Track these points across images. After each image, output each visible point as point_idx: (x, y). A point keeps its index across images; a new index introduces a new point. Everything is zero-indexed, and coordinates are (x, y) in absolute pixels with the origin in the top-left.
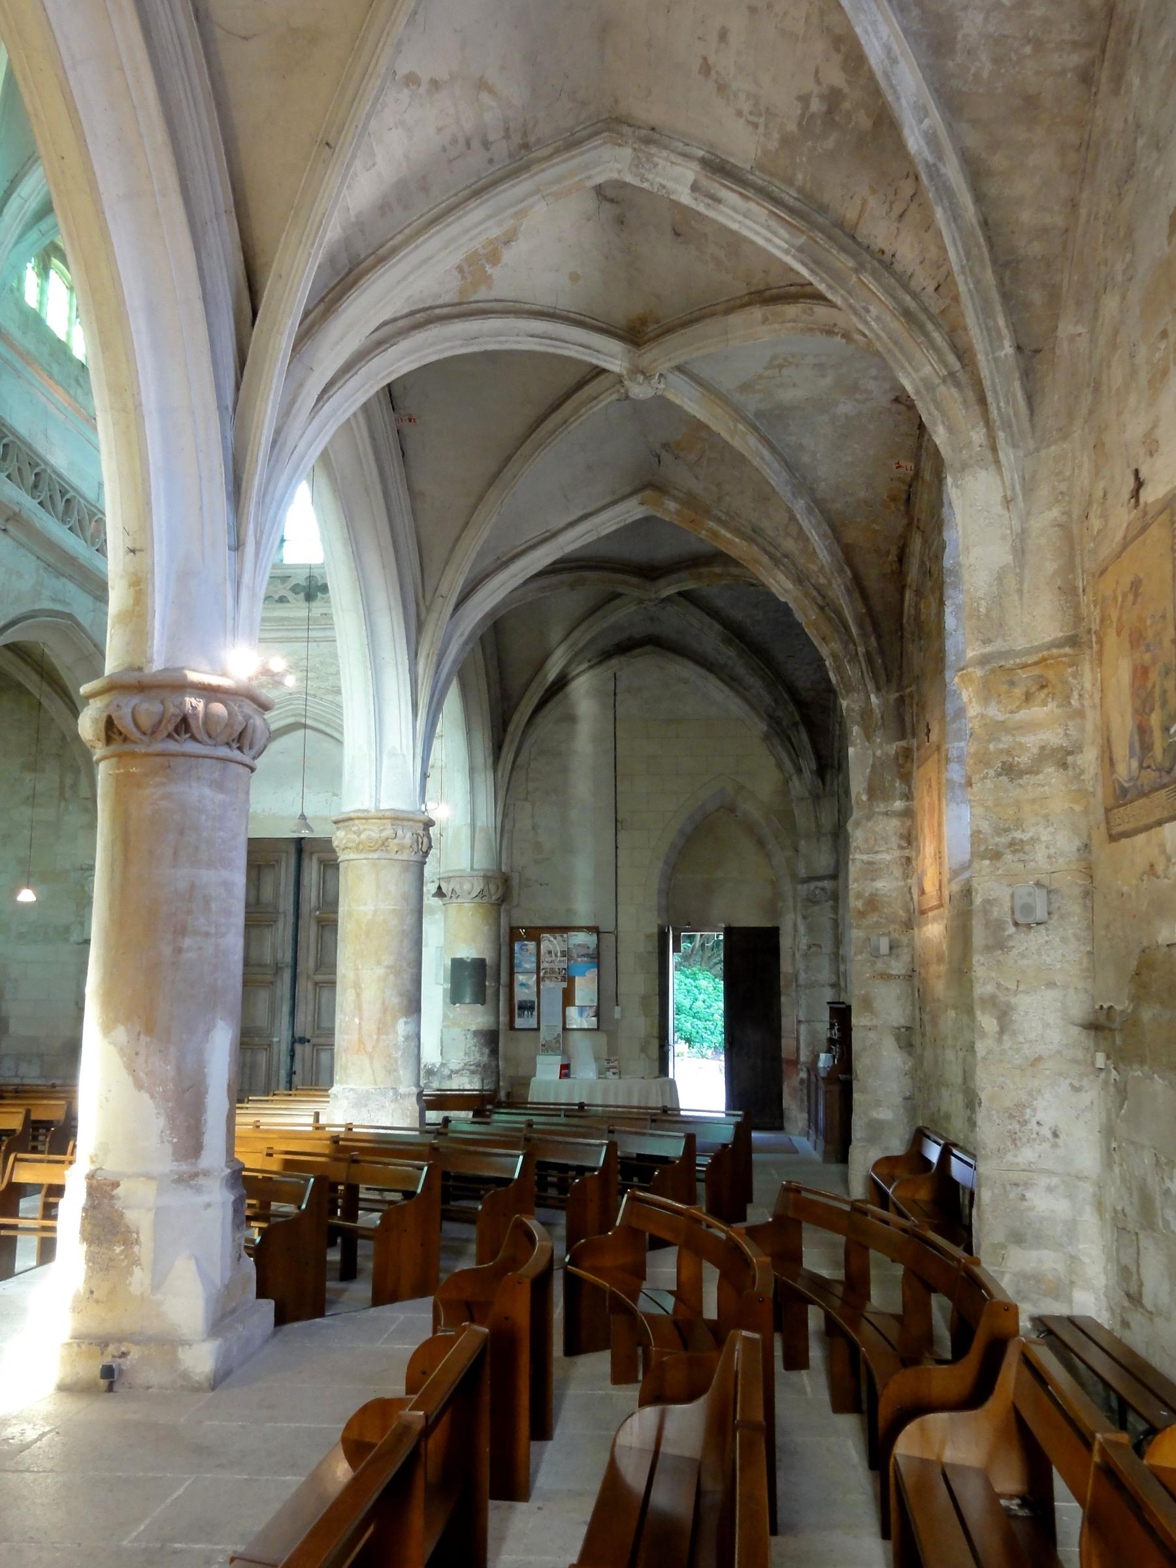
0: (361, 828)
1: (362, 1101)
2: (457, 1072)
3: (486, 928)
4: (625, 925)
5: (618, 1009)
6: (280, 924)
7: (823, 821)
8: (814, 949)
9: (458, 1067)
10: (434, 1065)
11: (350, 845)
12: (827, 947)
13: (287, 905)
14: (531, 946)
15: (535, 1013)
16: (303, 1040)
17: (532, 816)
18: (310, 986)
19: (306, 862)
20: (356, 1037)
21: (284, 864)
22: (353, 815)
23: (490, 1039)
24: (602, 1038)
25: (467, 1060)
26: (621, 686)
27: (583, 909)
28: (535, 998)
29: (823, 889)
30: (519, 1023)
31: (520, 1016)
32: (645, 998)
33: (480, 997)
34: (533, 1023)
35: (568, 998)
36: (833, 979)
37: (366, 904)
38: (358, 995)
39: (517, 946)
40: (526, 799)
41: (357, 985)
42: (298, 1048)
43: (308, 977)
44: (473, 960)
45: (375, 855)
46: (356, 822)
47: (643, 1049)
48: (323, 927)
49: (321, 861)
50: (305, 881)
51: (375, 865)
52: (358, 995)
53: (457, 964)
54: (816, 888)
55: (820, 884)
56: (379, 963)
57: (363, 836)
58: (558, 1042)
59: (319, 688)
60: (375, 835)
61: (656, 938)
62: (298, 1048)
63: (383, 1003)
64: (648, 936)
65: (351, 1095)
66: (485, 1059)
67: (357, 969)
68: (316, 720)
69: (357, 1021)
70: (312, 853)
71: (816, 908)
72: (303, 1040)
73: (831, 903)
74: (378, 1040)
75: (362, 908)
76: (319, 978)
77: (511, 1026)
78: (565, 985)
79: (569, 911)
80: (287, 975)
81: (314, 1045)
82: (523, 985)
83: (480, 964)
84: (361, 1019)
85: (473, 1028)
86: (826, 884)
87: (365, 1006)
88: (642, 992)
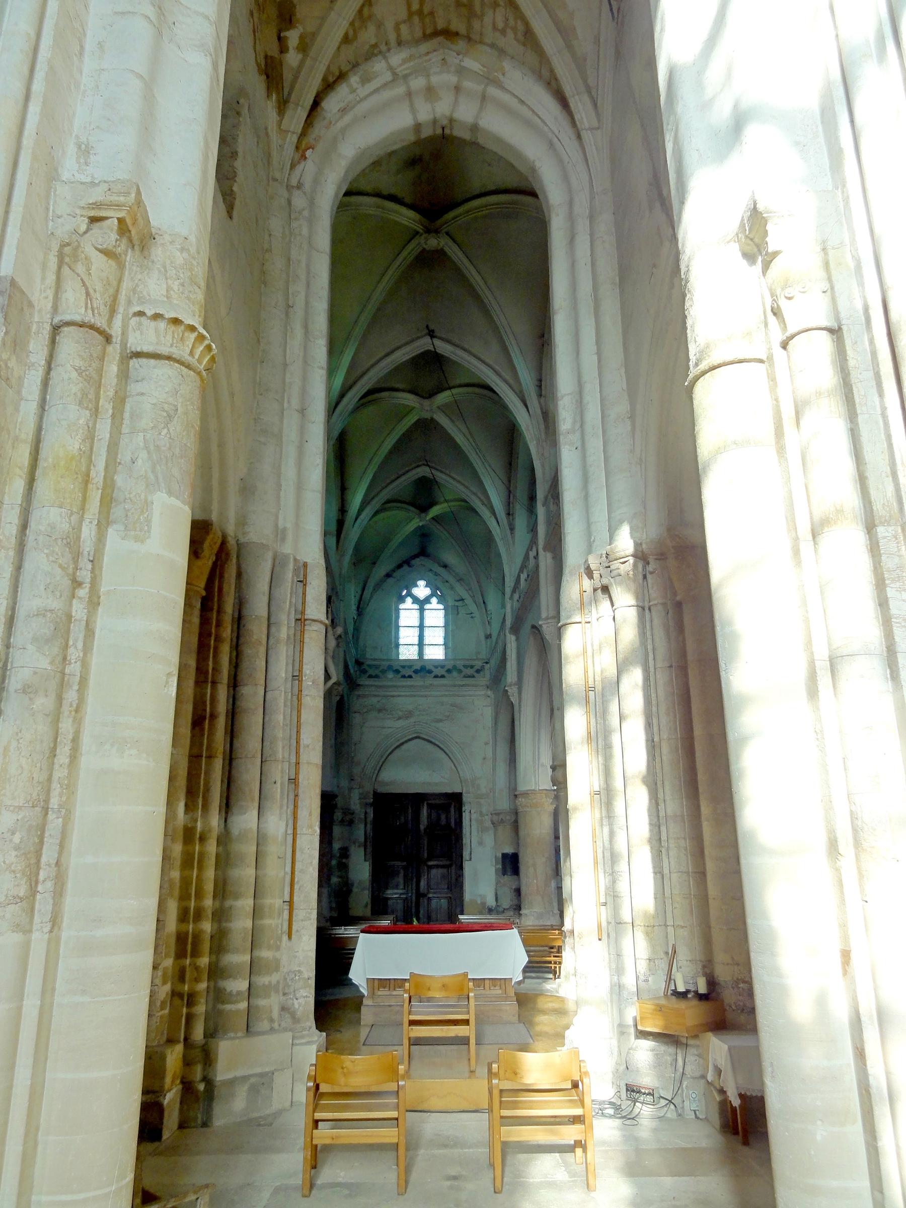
1: (540, 916)
38: (535, 870)
49: (428, 804)
53: (505, 856)
72: (424, 895)
76: (430, 863)
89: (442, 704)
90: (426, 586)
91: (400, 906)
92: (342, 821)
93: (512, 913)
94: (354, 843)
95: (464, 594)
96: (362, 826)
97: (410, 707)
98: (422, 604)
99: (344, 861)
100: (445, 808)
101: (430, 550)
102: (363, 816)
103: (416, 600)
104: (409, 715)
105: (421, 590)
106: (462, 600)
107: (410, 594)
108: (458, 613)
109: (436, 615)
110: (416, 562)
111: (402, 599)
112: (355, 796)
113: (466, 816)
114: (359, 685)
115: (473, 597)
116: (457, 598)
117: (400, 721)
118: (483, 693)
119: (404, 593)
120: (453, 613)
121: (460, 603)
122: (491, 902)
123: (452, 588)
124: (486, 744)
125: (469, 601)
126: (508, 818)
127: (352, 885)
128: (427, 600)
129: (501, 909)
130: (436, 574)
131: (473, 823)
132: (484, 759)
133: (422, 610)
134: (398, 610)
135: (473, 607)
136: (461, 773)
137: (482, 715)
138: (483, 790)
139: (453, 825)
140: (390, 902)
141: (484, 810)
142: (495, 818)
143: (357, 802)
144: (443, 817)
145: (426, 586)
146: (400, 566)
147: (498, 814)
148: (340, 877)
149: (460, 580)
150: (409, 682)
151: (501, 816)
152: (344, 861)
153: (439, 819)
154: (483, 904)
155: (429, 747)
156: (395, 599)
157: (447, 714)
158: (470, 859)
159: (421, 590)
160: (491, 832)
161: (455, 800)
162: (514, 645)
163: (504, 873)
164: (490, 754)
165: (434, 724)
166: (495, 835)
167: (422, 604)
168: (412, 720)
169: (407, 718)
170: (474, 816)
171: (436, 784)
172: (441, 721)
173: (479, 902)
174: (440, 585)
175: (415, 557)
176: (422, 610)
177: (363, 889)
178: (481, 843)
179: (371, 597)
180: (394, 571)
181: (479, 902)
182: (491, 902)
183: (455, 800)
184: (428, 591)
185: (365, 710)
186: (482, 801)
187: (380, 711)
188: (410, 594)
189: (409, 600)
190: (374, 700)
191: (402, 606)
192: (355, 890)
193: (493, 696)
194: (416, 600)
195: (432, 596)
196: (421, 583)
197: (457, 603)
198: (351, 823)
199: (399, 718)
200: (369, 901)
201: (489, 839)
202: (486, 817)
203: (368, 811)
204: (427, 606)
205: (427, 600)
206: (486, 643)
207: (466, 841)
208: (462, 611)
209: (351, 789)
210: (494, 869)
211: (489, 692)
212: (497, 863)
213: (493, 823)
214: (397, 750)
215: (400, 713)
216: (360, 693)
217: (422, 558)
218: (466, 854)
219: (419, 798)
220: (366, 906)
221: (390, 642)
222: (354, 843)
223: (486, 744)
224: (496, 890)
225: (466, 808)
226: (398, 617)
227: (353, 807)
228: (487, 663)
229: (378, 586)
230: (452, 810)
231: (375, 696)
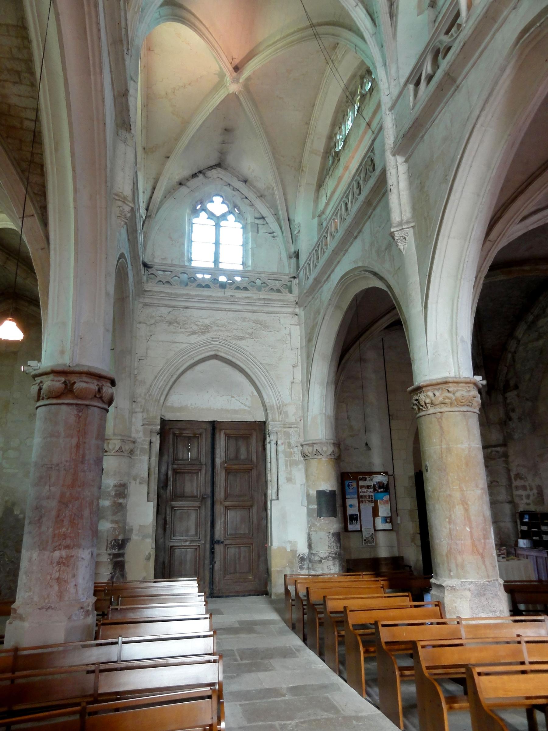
0: (456, 389)
2: (325, 558)
3: (333, 473)
4: (399, 472)
5: (399, 518)
6: (203, 471)
7: (491, 416)
8: (494, 483)
9: (325, 555)
10: (304, 554)
11: (447, 401)
12: (503, 481)
13: (205, 459)
14: (354, 484)
15: (359, 521)
16: (218, 542)
17: (347, 411)
18: (222, 509)
19: (217, 436)
20: (469, 542)
21: (204, 436)
22: (450, 380)
23: (338, 536)
24: (394, 535)
25: (330, 550)
26: (386, 346)
27: (377, 461)
28: (357, 513)
29: (497, 452)
30: (351, 527)
31: (350, 524)
32: (411, 511)
33: (334, 514)
34: (357, 527)
35: (375, 513)
36: (509, 498)
37: (462, 443)
38: (466, 510)
39: (347, 483)
40: (343, 402)
41: (464, 502)
42: (216, 547)
43: (221, 503)
44: (330, 491)
45: (465, 409)
46: (450, 385)
47: (413, 540)
48: (229, 473)
49: (226, 435)
50: (217, 446)
51: (465, 416)
52: (466, 510)
54: (492, 452)
55: (494, 449)
56: (477, 486)
57: (458, 394)
58: (372, 538)
59: (228, 336)
60: (466, 394)
61: (414, 478)
62: (216, 547)
63: (484, 516)
64: (410, 477)
65: (472, 587)
66: (338, 550)
67: (462, 490)
68: (226, 354)
69: (468, 529)
70: (221, 430)
71: (493, 462)
72: (218, 542)
73: (503, 459)
74: (485, 543)
75: (459, 446)
76: (227, 503)
77: (346, 529)
78: (373, 505)
79: (371, 464)
80: (209, 502)
81: (226, 545)
82: (351, 506)
83: (332, 493)
84: (471, 528)
85: (332, 531)
86: (499, 449)
87: (473, 518)
88: (409, 508)
89: (244, 320)
90: (223, 202)
91: (190, 554)
92: (120, 450)
93: (331, 563)
94: (135, 479)
95: (265, 212)
96: (146, 458)
97: (207, 322)
98: (218, 220)
99: (121, 501)
100: (246, 438)
101: (230, 159)
102: (147, 447)
103: (211, 215)
104: (206, 329)
105: (217, 206)
106: (263, 218)
107: (204, 209)
108: (258, 232)
109: (233, 232)
110: (213, 173)
111: (195, 212)
112: (138, 421)
113: (271, 449)
114: (146, 291)
115: (276, 215)
116: (257, 215)
117: (195, 336)
118: (290, 310)
119: (199, 207)
120: (255, 227)
121: (260, 222)
122: (303, 549)
123: (252, 205)
124: (294, 366)
125: (270, 219)
126: (325, 449)
127: (131, 530)
128: (224, 217)
129: (317, 558)
130: (235, 189)
131: (281, 455)
132: (293, 382)
133: (217, 226)
134: (191, 224)
135: (274, 226)
136: (265, 397)
137: (290, 334)
138: (292, 419)
139: (254, 458)
140: (177, 551)
141: (293, 440)
142: (308, 450)
143: (140, 428)
144: (243, 450)
145: (223, 202)
146: (194, 176)
147: (312, 445)
148: (113, 522)
149: (261, 196)
150: (206, 292)
151: (316, 447)
152: (121, 501)
153: (238, 450)
154: (294, 552)
155: (228, 369)
156: (188, 211)
157: (250, 331)
158: (278, 499)
159: (217, 206)
160: (301, 466)
161: (256, 432)
162: (403, 168)
163: (320, 515)
164: (299, 376)
165: (235, 342)
166: (306, 470)
167: (218, 220)
168: (208, 336)
169: (203, 333)
170: (281, 448)
171: (236, 412)
172: (242, 338)
173: (289, 550)
174: (238, 202)
175: (211, 168)
176: (217, 226)
177: (145, 536)
178: (289, 480)
179: (162, 202)
180: (188, 180)
181: (289, 550)
182: (303, 549)
183: (256, 432)
184: (224, 209)
185: (153, 321)
186: (291, 431)
187: (170, 323)
188: (204, 209)
189: (203, 215)
190: (164, 311)
191: (195, 220)
192: (134, 537)
193: (302, 313)
194: (211, 215)
195: (230, 212)
196: (218, 200)
197: (257, 221)
198: (132, 452)
199: (194, 333)
200: (153, 552)
201: (299, 475)
202: (296, 449)
203: (153, 440)
204: (223, 223)
205: (224, 217)
206: (289, 264)
207: (271, 475)
208: (262, 230)
209: (132, 412)
210: (305, 510)
211: (297, 310)
212: (309, 503)
213: (305, 456)
214: (189, 372)
215: (195, 328)
216: (147, 301)
217: (219, 169)
218: (271, 492)
219: (214, 426)
220: (148, 559)
221: (183, 255)
222: (135, 479)
223: (294, 366)
224: (309, 535)
225: (272, 439)
226: (191, 231)
227: (133, 435)
228: (294, 278)
229: (169, 193)
230: (254, 441)
231: (166, 306)
